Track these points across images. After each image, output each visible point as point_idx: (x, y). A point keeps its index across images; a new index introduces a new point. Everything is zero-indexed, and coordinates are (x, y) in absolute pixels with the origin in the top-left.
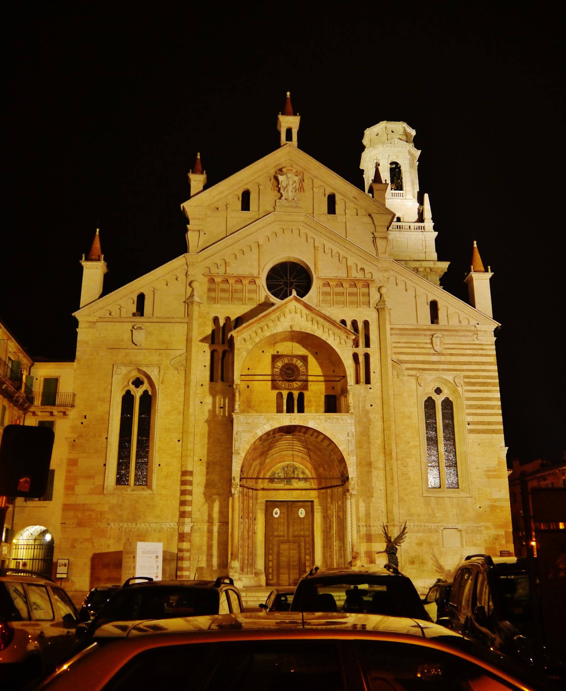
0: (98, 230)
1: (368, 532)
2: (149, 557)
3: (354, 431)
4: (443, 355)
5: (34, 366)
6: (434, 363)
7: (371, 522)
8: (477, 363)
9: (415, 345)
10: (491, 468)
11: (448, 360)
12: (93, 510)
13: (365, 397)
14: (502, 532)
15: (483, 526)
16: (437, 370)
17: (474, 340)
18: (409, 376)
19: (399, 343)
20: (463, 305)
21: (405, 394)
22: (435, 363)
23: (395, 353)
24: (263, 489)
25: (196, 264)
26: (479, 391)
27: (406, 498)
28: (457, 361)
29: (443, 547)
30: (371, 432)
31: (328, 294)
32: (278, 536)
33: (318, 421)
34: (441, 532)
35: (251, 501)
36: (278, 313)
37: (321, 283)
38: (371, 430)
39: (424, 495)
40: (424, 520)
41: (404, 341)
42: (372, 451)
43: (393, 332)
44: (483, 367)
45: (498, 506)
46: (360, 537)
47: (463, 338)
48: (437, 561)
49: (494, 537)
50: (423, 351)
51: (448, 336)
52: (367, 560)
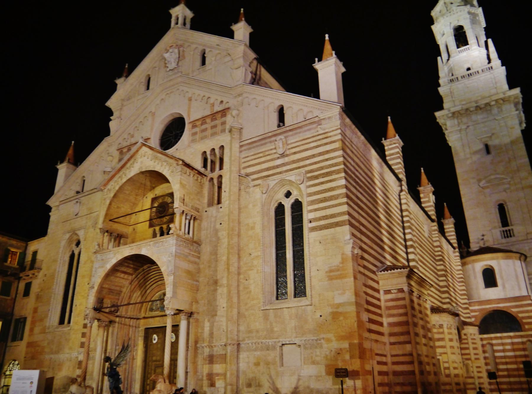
0: (73, 142)
1: (211, 353)
2: (23, 383)
3: (174, 250)
4: (287, 155)
5: (29, 245)
6: (278, 167)
7: (214, 341)
8: (321, 154)
9: (261, 155)
10: (334, 268)
11: (292, 160)
12: (39, 346)
13: (216, 217)
14: (345, 345)
15: (323, 338)
16: (280, 173)
17: (318, 131)
18: (254, 186)
19: (248, 157)
20: (305, 99)
21: (251, 206)
22: (279, 167)
23: (245, 168)
24: (144, 318)
25: (113, 143)
26: (322, 183)
27: (246, 313)
28: (300, 158)
29: (282, 365)
30: (219, 250)
31: (195, 134)
32: (156, 361)
33: (149, 247)
34: (278, 348)
35: (131, 329)
36: (131, 162)
37: (191, 126)
38: (219, 248)
39: (262, 309)
40: (262, 336)
41: (252, 153)
42: (218, 269)
43: (243, 148)
44: (326, 156)
45: (341, 313)
46: (204, 359)
47: (307, 133)
48: (273, 383)
49: (336, 352)
50: (269, 158)
51: (292, 135)
52: (208, 383)
